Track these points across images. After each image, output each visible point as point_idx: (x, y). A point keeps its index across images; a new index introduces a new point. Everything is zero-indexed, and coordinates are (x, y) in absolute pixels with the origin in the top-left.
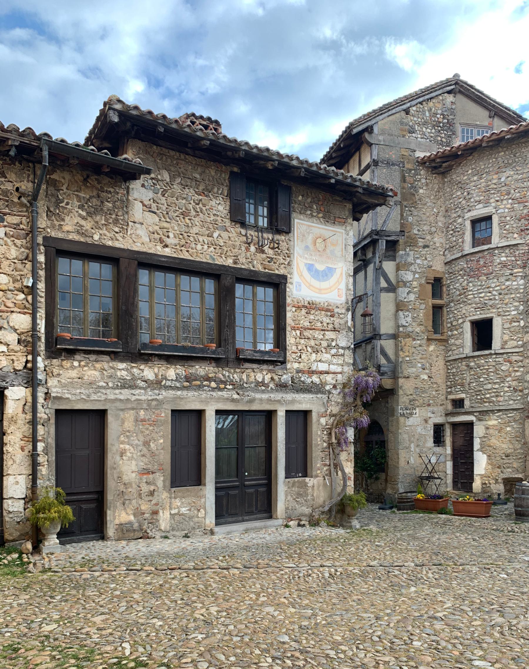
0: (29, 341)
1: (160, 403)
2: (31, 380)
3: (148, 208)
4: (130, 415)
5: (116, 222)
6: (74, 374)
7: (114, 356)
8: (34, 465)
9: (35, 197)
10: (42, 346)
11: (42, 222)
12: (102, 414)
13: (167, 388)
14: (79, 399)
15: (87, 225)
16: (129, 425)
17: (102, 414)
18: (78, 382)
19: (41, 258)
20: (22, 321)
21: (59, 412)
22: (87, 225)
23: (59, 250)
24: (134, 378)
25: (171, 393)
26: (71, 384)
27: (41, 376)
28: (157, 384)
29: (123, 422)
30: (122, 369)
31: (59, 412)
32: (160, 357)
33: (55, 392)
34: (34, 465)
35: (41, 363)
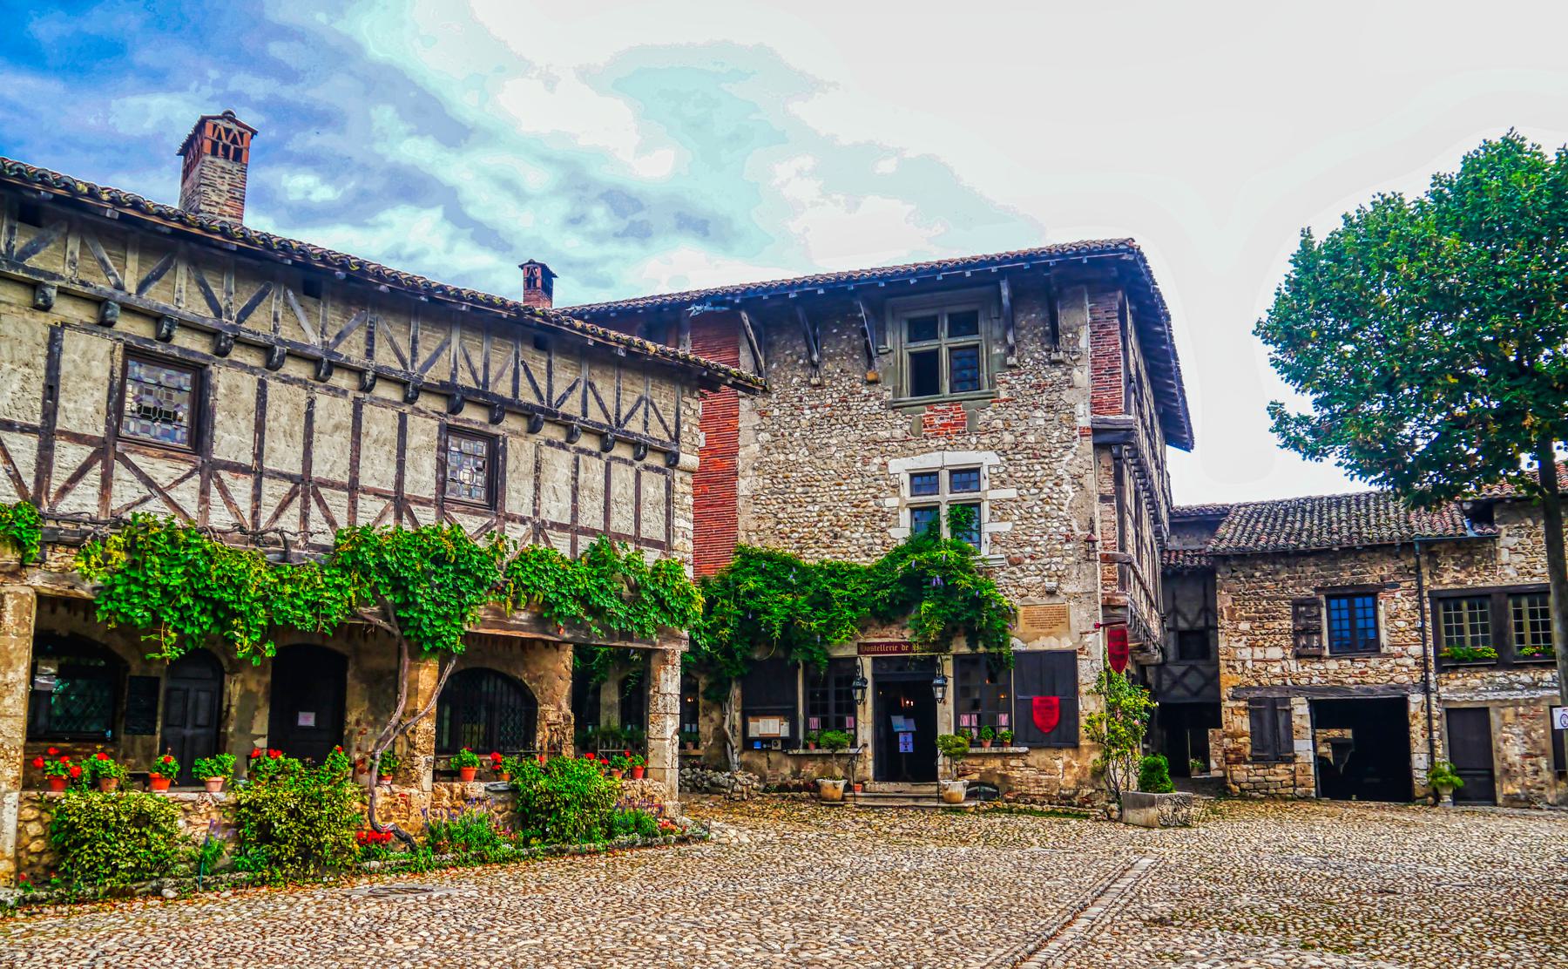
0: (1423, 664)
1: (1538, 701)
2: (1426, 689)
3: (1513, 551)
4: (1510, 711)
5: (1486, 568)
6: (1458, 682)
7: (1492, 667)
8: (1432, 746)
9: (1418, 568)
10: (1432, 665)
11: (1426, 582)
12: (1484, 712)
13: (1543, 688)
14: (1461, 699)
15: (1461, 576)
16: (1510, 718)
17: (1484, 712)
18: (1463, 688)
19: (1428, 606)
20: (1416, 650)
21: (1448, 711)
22: (1461, 576)
23: (1438, 598)
24: (1511, 682)
25: (1547, 693)
26: (1457, 690)
27: (1433, 686)
28: (1534, 685)
29: (1504, 716)
30: (1500, 677)
31: (1448, 711)
32: (1535, 664)
33: (1444, 696)
34: (1432, 746)
35: (1432, 677)
